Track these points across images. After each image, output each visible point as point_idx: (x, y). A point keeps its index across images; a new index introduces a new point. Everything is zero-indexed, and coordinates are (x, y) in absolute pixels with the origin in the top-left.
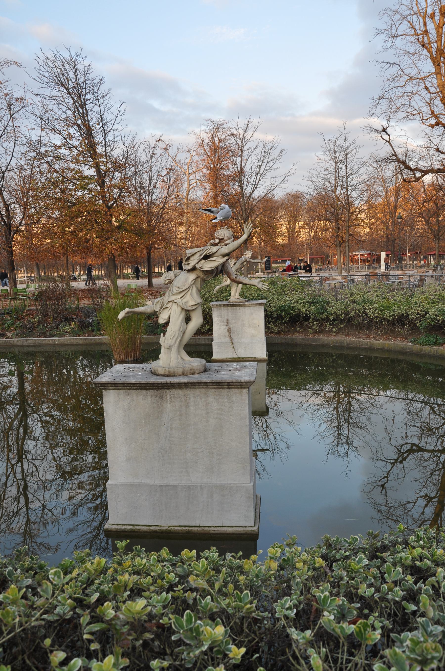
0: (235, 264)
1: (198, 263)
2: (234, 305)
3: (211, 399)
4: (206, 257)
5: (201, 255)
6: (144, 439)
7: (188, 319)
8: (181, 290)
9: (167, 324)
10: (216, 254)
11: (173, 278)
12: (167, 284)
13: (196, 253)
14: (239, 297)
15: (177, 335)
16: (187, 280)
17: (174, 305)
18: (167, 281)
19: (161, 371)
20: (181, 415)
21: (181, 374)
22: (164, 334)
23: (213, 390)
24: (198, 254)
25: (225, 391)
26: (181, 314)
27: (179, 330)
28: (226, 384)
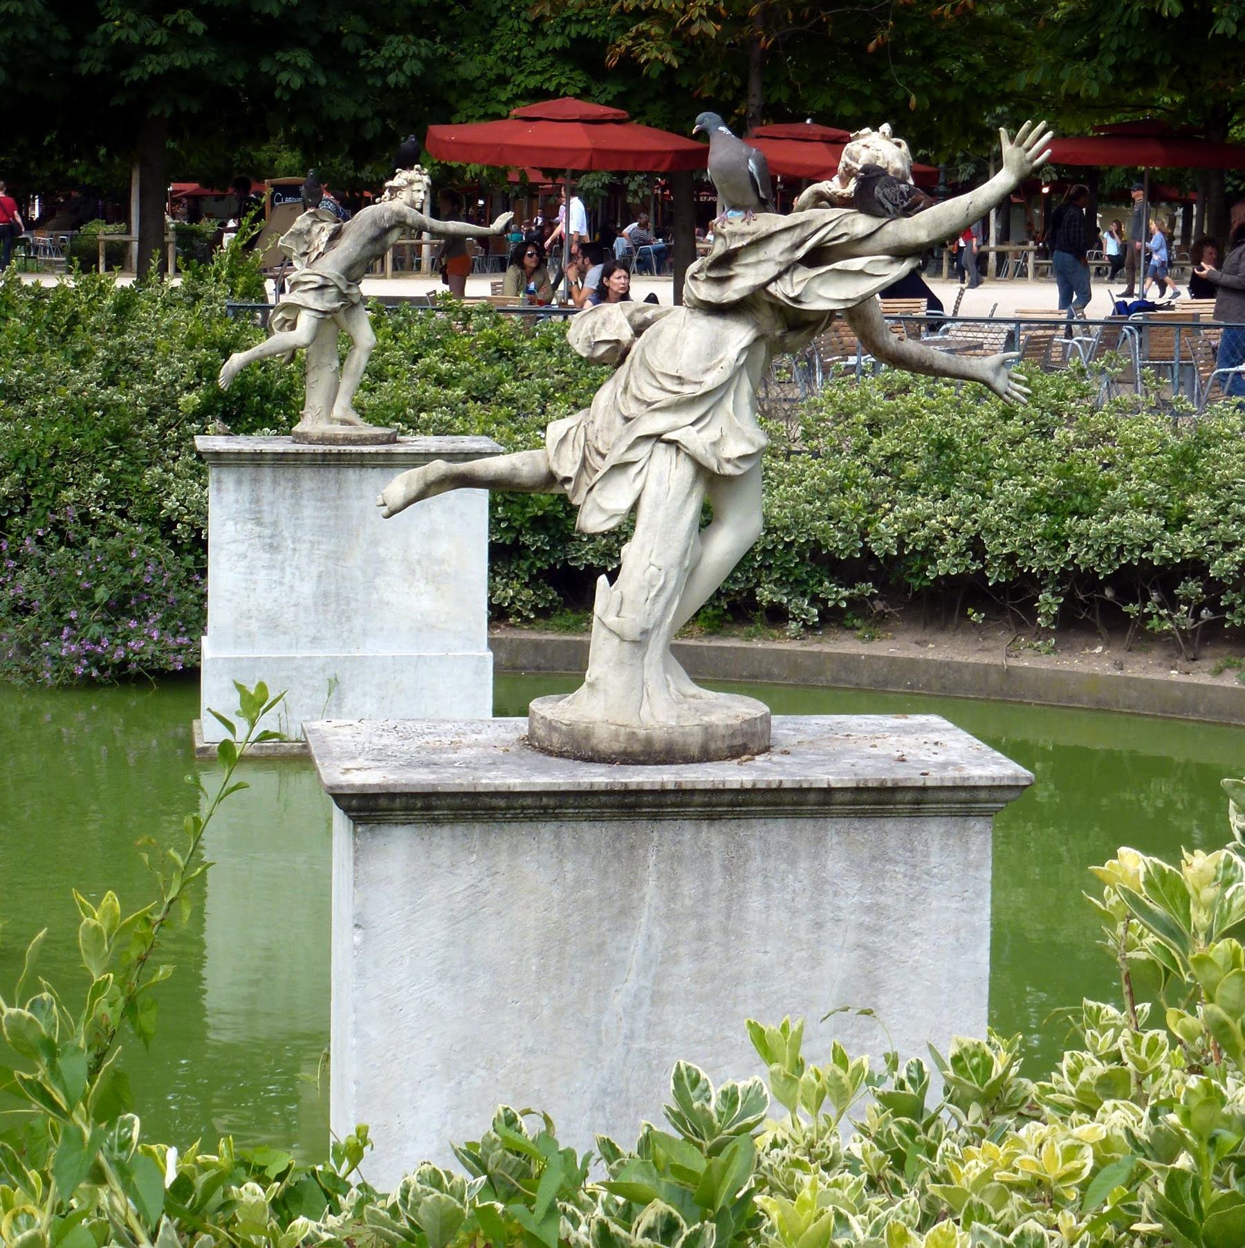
0: (335, 236)
1: (775, 279)
2: (334, 460)
3: (835, 864)
4: (818, 256)
5: (797, 246)
6: (532, 1051)
7: (707, 519)
8: (688, 390)
9: (621, 534)
10: (870, 245)
11: (626, 334)
12: (600, 361)
13: (770, 237)
14: (353, 416)
15: (672, 584)
16: (715, 347)
17: (663, 455)
18: (602, 350)
19: (603, 739)
20: (702, 936)
21: (695, 750)
22: (613, 577)
23: (843, 824)
24: (785, 242)
25: (892, 832)
26: (689, 494)
27: (681, 563)
28: (909, 796)
